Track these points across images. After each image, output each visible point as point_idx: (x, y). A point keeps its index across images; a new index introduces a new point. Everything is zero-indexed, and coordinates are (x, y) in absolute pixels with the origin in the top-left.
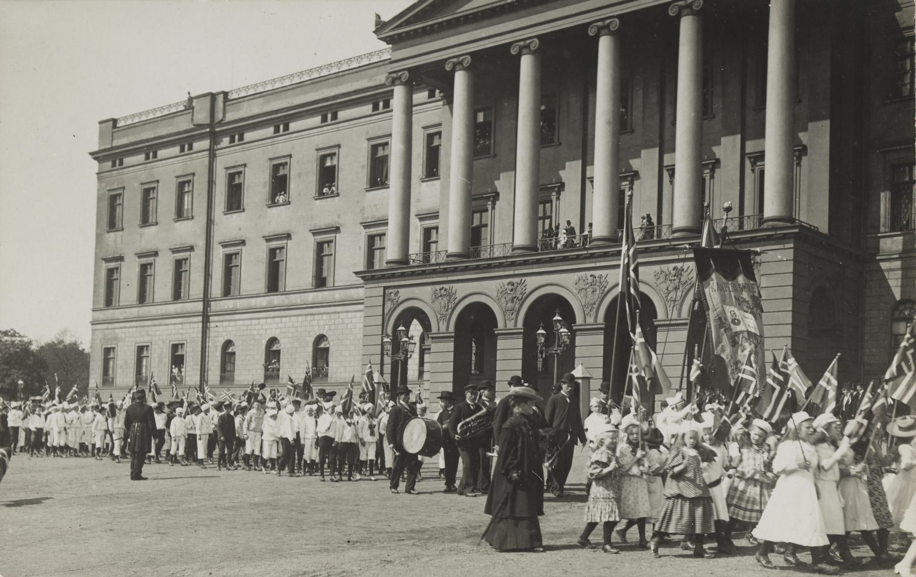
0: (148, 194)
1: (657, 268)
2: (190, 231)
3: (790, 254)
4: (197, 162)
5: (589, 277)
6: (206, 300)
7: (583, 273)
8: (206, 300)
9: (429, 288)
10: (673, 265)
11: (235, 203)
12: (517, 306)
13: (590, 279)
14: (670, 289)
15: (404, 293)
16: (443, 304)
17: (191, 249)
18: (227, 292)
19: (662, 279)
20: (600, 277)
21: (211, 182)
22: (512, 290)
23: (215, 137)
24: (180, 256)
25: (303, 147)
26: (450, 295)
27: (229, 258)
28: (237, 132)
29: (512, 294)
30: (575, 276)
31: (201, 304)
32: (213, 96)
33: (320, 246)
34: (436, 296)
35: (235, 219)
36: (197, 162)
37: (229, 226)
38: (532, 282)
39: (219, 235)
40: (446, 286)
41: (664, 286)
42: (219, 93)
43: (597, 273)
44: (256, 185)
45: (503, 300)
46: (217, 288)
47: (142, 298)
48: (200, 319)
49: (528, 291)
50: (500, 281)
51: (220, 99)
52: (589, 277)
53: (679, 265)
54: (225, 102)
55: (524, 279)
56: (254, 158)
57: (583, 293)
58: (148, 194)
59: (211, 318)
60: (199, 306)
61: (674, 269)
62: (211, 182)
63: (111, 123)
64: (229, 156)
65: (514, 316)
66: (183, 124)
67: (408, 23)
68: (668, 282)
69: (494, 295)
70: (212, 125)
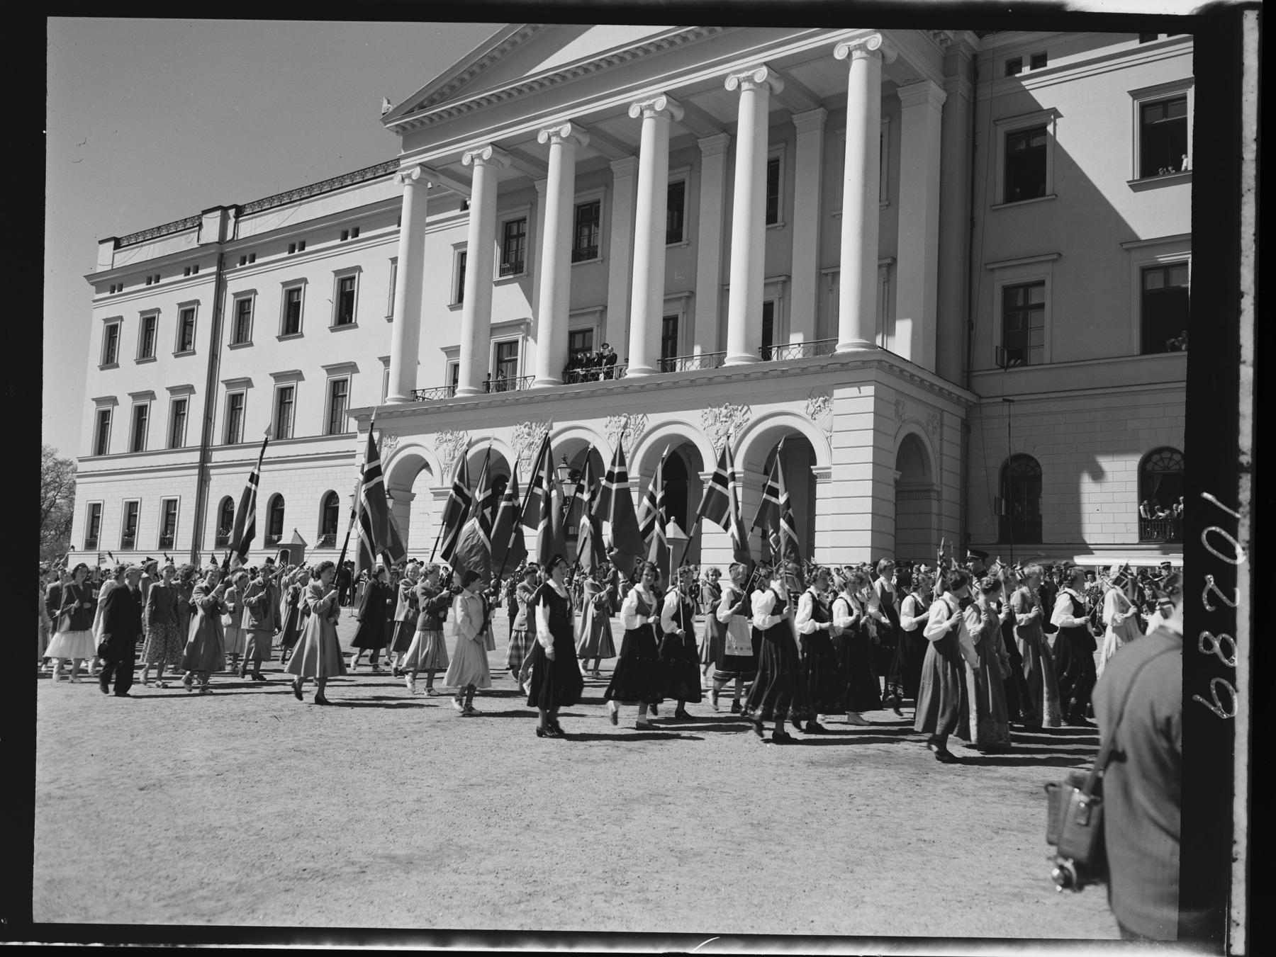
0: (149, 324)
4: (203, 292)
11: (242, 337)
14: (721, 433)
17: (190, 389)
18: (232, 438)
19: (710, 421)
22: (529, 434)
24: (179, 397)
29: (530, 440)
31: (198, 454)
32: (224, 209)
37: (233, 364)
42: (231, 207)
44: (268, 314)
46: (218, 437)
47: (138, 444)
48: (196, 471)
51: (232, 212)
54: (237, 217)
56: (265, 285)
58: (149, 324)
59: (212, 472)
60: (196, 457)
63: (112, 244)
64: (237, 284)
67: (422, 107)
68: (718, 424)
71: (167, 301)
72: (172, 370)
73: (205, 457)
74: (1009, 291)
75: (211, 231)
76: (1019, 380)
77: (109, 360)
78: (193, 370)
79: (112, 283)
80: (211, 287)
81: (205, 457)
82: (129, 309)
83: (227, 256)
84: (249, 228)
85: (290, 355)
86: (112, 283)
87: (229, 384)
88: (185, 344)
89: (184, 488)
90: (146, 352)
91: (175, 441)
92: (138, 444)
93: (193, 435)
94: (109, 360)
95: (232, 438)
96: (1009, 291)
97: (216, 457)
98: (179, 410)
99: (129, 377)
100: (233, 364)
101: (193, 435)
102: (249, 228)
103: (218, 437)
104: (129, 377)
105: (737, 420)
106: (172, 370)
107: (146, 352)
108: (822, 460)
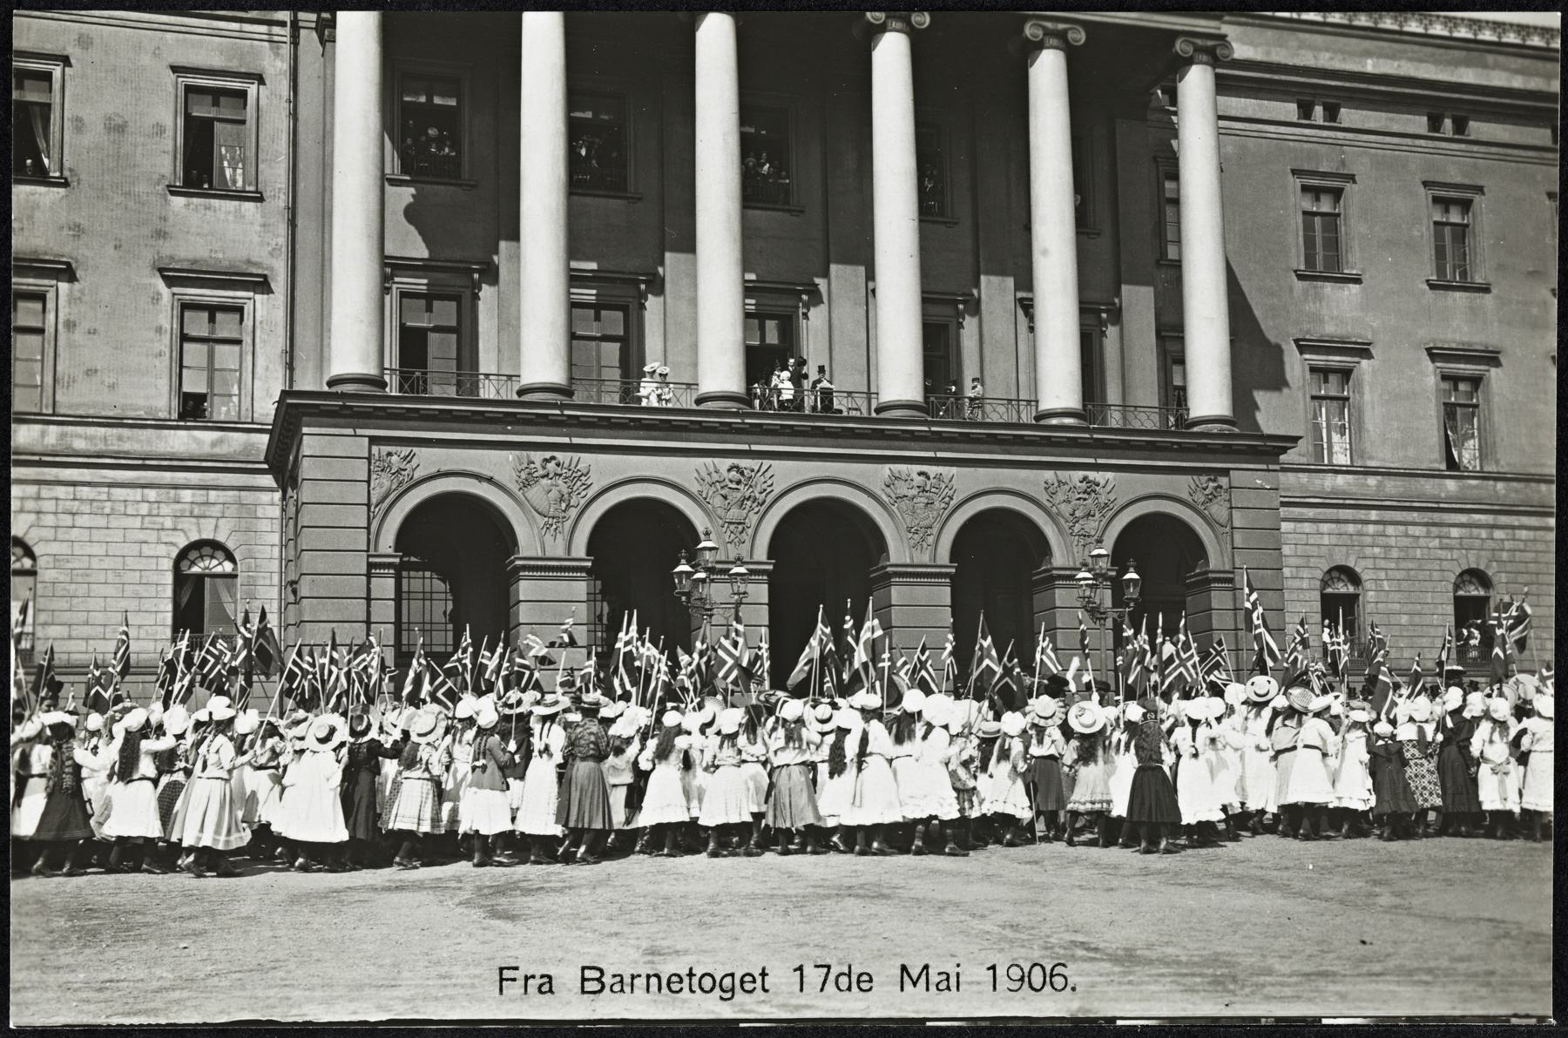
1: (1049, 475)
5: (915, 476)
7: (903, 467)
9: (511, 455)
10: (1081, 474)
12: (754, 519)
13: (919, 480)
14: (1077, 514)
16: (554, 494)
20: (939, 477)
22: (739, 482)
26: (577, 477)
30: (886, 469)
40: (560, 455)
41: (1065, 509)
43: (932, 470)
45: (718, 501)
49: (777, 490)
50: (708, 460)
52: (915, 476)
53: (1092, 475)
55: (767, 463)
57: (905, 504)
61: (1085, 478)
65: (747, 537)
69: (694, 488)
105: (1103, 499)
108: (1216, 560)
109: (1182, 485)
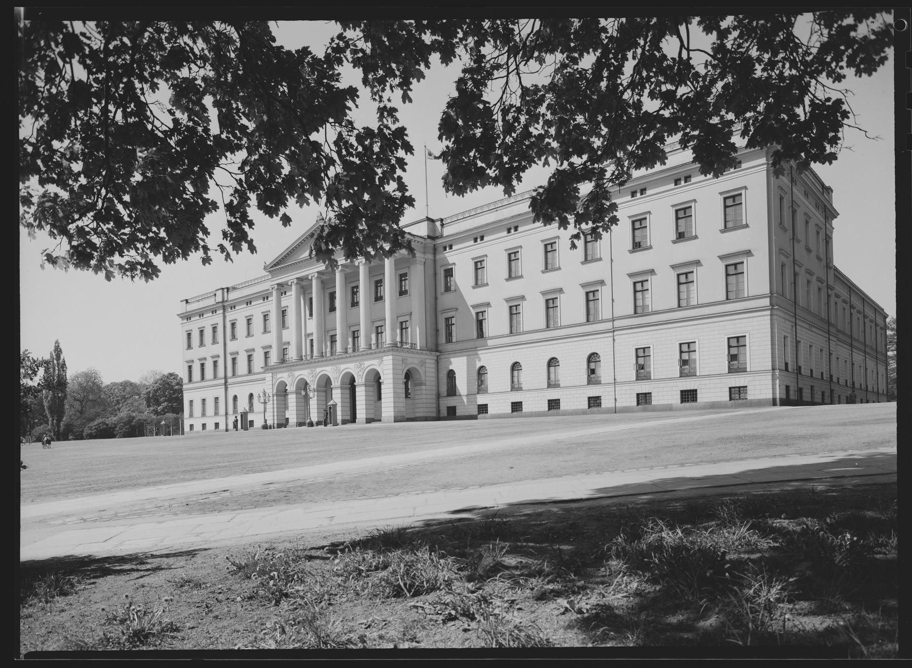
0: (202, 332)
2: (218, 349)
3: (391, 357)
6: (226, 377)
8: (226, 377)
11: (234, 337)
15: (279, 375)
17: (218, 356)
18: (234, 374)
21: (224, 327)
23: (224, 308)
25: (257, 310)
27: (234, 360)
28: (233, 307)
33: (266, 353)
34: (289, 376)
35: (234, 342)
36: (218, 319)
37: (232, 346)
38: (318, 370)
39: (229, 350)
46: (230, 373)
47: (203, 378)
56: (239, 315)
58: (202, 332)
60: (223, 381)
62: (224, 327)
64: (231, 315)
66: (211, 301)
67: (275, 265)
70: (223, 301)
71: (207, 322)
72: (212, 350)
73: (226, 382)
74: (447, 319)
75: (219, 298)
76: (450, 347)
77: (189, 346)
78: (218, 349)
79: (187, 317)
80: (222, 318)
81: (226, 382)
82: (195, 325)
83: (225, 306)
84: (233, 296)
85: (250, 343)
86: (187, 317)
87: (231, 354)
88: (215, 341)
89: (220, 392)
90: (202, 344)
91: (215, 377)
92: (203, 378)
93: (221, 373)
94: (189, 346)
95: (234, 374)
96: (447, 319)
97: (229, 381)
98: (215, 363)
99: (197, 353)
100: (232, 346)
101: (221, 373)
102: (233, 296)
103: (230, 373)
104: (197, 353)
106: (212, 350)
107: (202, 344)
109: (376, 362)
